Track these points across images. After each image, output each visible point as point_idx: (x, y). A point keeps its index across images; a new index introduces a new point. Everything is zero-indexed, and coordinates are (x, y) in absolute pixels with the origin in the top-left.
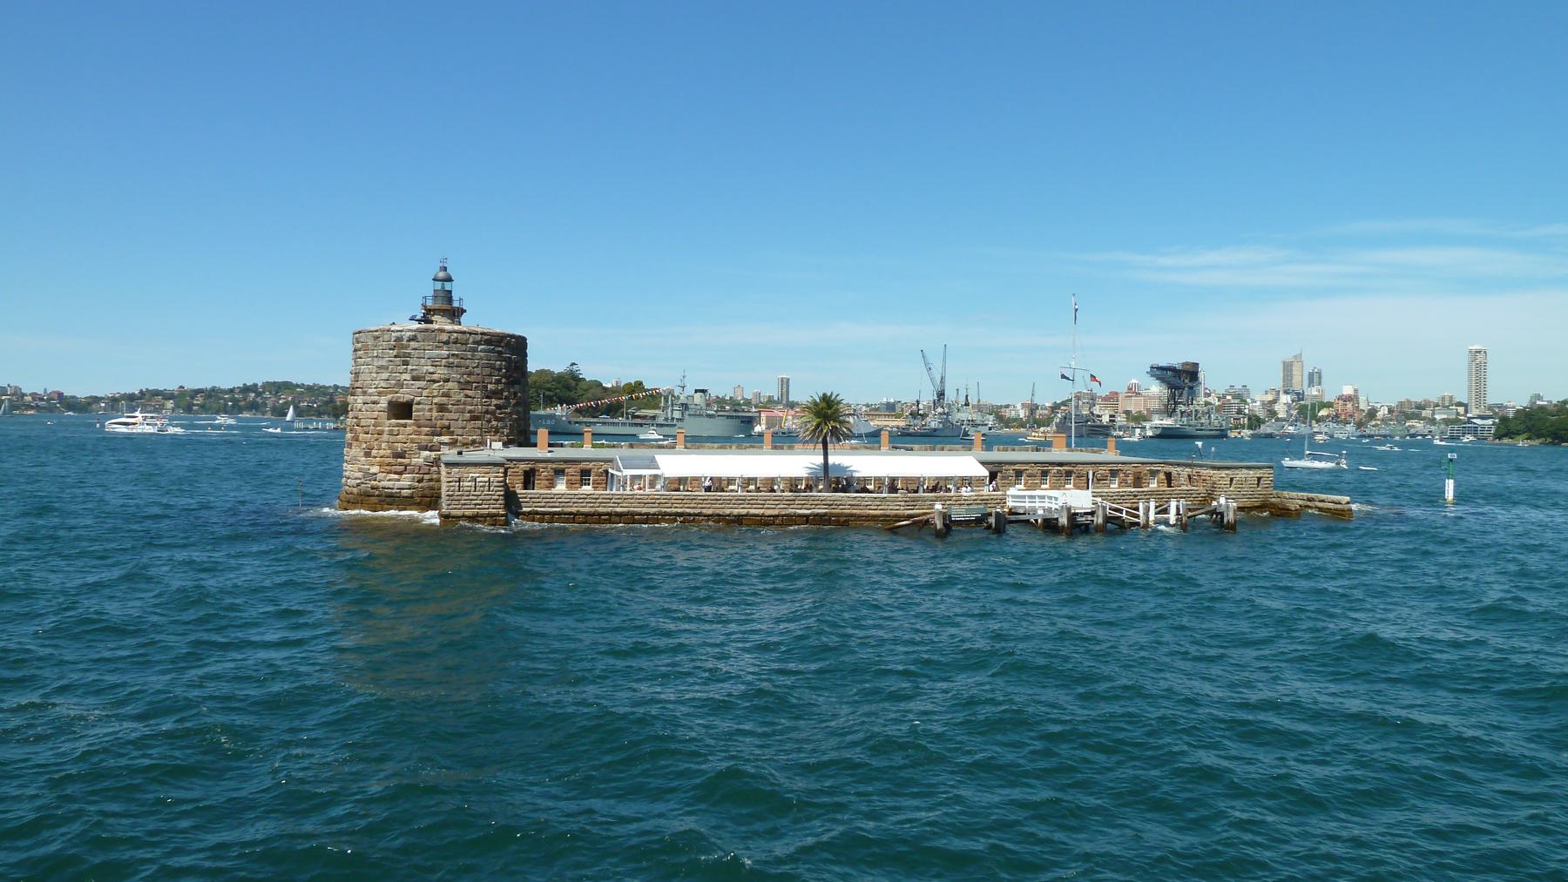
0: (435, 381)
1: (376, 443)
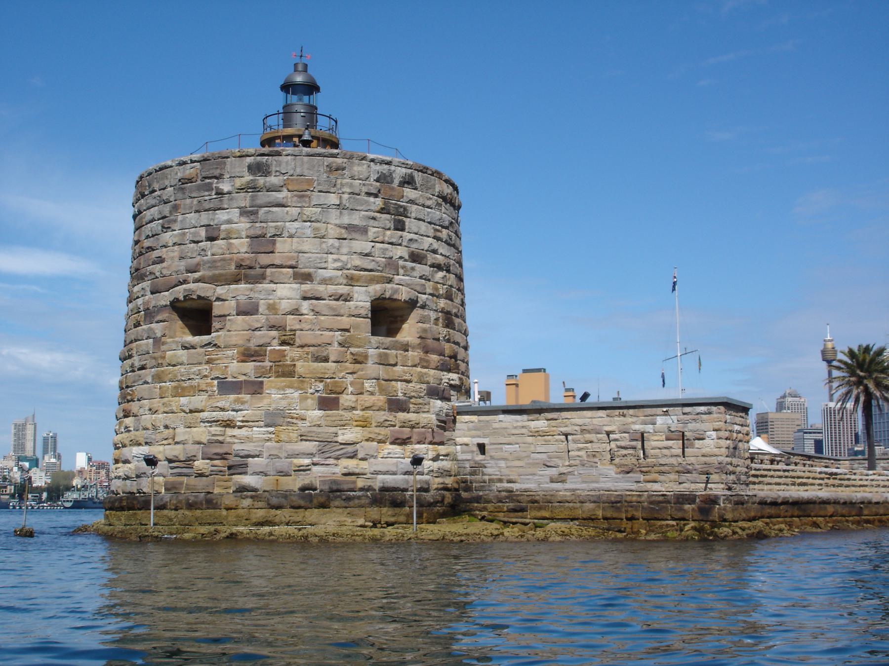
1: (350, 378)
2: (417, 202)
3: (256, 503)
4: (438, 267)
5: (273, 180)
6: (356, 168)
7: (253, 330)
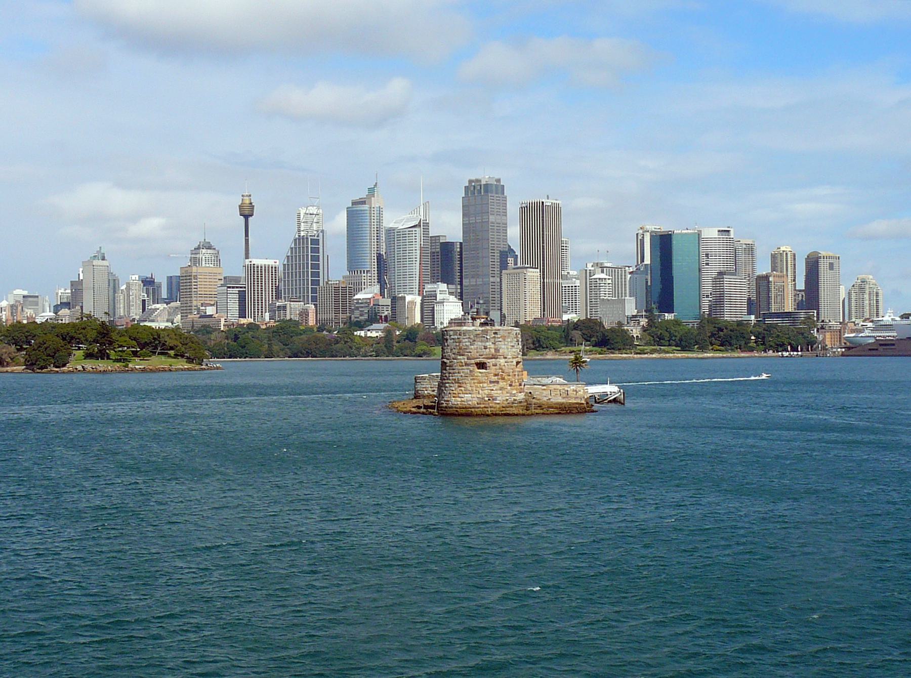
5: (499, 336)
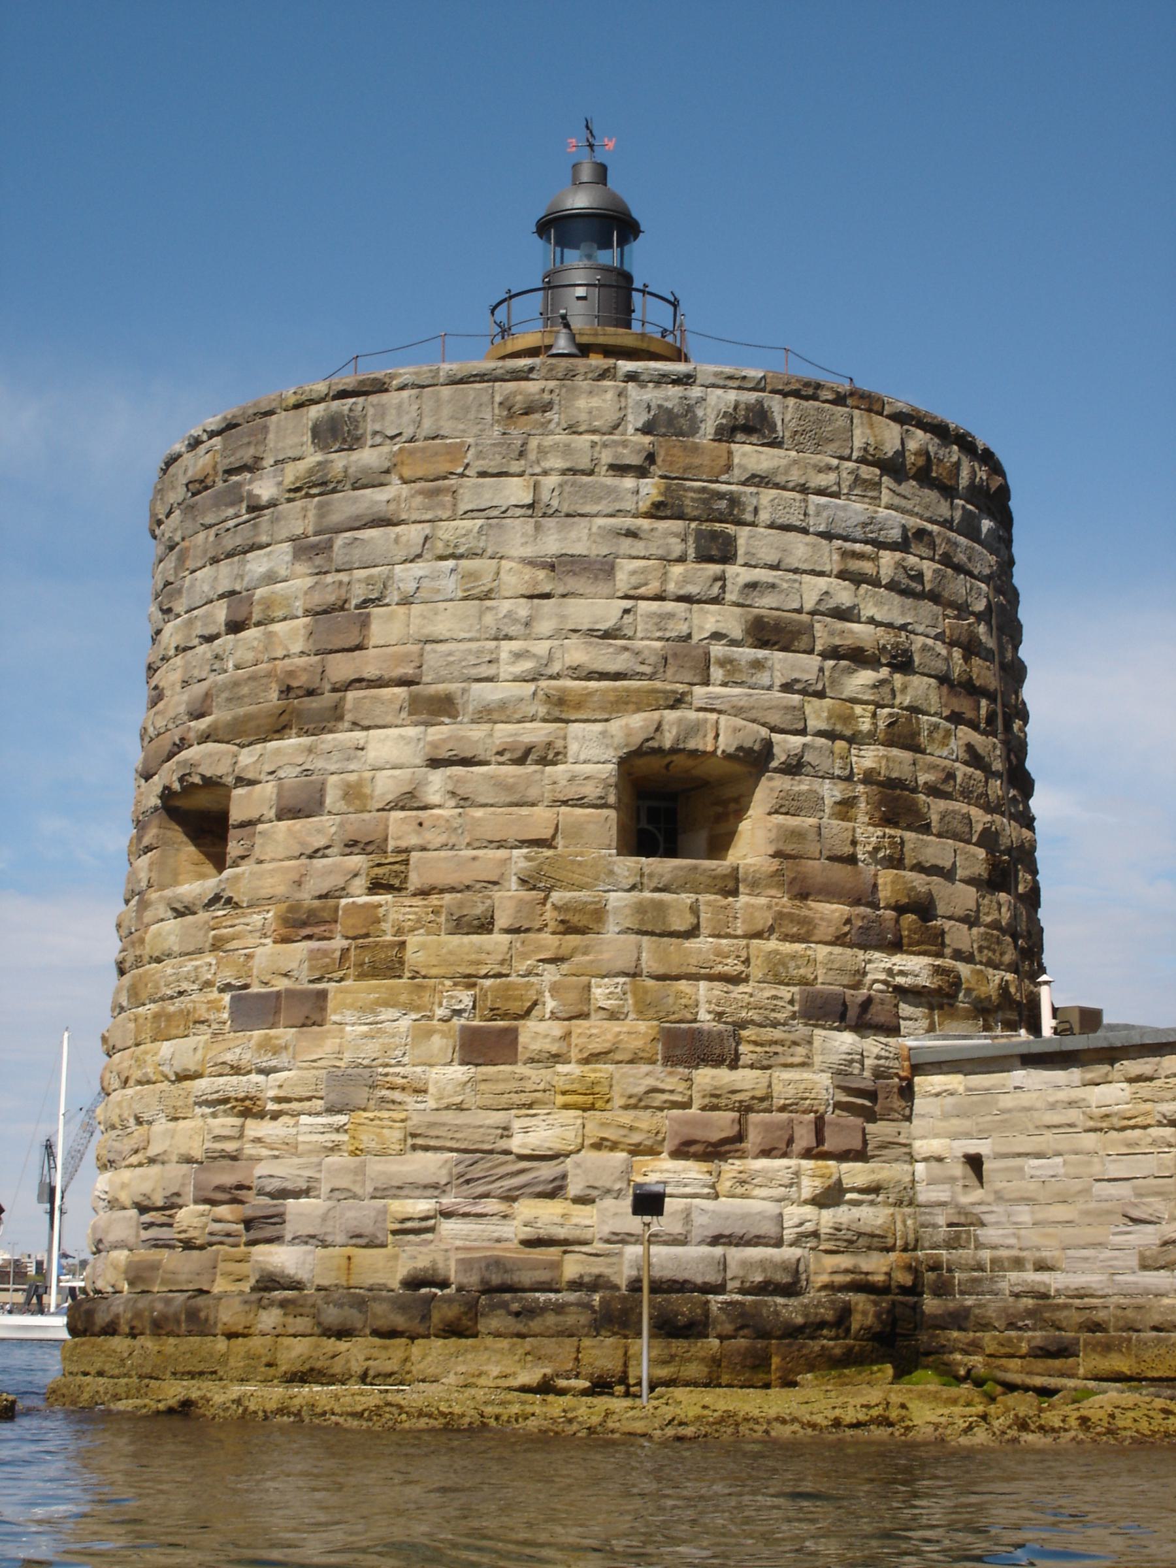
0: (858, 657)
1: (551, 974)
2: (780, 479)
3: (290, 1320)
4: (858, 657)
6: (582, 403)
7: (310, 857)
